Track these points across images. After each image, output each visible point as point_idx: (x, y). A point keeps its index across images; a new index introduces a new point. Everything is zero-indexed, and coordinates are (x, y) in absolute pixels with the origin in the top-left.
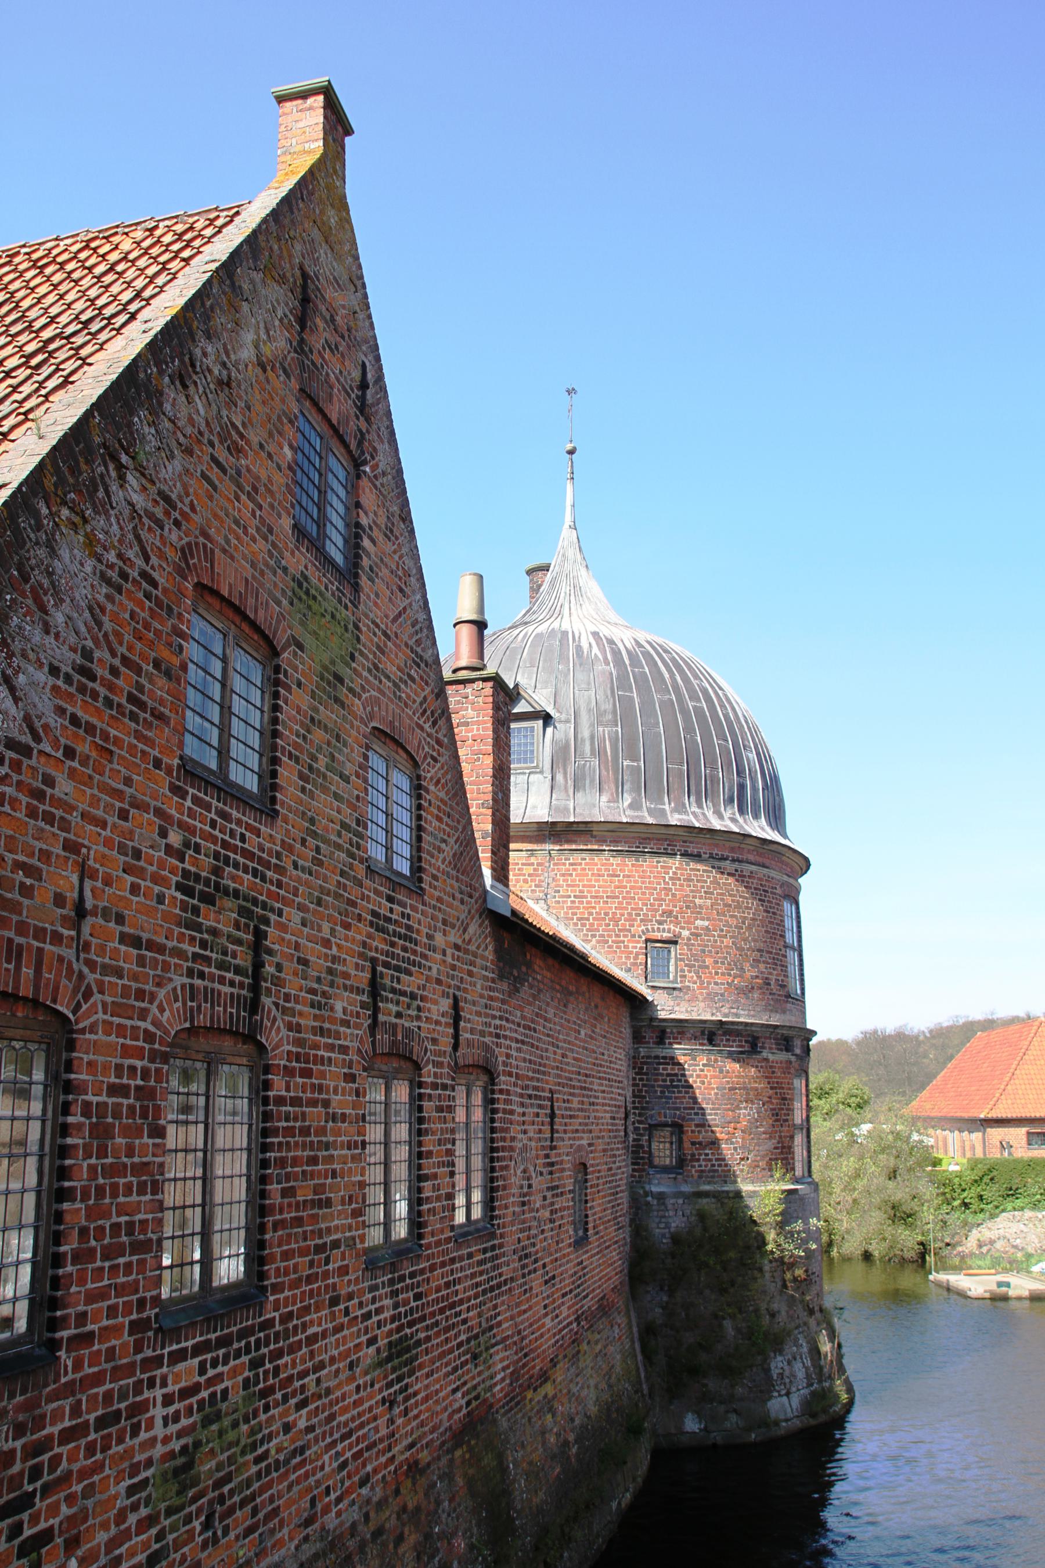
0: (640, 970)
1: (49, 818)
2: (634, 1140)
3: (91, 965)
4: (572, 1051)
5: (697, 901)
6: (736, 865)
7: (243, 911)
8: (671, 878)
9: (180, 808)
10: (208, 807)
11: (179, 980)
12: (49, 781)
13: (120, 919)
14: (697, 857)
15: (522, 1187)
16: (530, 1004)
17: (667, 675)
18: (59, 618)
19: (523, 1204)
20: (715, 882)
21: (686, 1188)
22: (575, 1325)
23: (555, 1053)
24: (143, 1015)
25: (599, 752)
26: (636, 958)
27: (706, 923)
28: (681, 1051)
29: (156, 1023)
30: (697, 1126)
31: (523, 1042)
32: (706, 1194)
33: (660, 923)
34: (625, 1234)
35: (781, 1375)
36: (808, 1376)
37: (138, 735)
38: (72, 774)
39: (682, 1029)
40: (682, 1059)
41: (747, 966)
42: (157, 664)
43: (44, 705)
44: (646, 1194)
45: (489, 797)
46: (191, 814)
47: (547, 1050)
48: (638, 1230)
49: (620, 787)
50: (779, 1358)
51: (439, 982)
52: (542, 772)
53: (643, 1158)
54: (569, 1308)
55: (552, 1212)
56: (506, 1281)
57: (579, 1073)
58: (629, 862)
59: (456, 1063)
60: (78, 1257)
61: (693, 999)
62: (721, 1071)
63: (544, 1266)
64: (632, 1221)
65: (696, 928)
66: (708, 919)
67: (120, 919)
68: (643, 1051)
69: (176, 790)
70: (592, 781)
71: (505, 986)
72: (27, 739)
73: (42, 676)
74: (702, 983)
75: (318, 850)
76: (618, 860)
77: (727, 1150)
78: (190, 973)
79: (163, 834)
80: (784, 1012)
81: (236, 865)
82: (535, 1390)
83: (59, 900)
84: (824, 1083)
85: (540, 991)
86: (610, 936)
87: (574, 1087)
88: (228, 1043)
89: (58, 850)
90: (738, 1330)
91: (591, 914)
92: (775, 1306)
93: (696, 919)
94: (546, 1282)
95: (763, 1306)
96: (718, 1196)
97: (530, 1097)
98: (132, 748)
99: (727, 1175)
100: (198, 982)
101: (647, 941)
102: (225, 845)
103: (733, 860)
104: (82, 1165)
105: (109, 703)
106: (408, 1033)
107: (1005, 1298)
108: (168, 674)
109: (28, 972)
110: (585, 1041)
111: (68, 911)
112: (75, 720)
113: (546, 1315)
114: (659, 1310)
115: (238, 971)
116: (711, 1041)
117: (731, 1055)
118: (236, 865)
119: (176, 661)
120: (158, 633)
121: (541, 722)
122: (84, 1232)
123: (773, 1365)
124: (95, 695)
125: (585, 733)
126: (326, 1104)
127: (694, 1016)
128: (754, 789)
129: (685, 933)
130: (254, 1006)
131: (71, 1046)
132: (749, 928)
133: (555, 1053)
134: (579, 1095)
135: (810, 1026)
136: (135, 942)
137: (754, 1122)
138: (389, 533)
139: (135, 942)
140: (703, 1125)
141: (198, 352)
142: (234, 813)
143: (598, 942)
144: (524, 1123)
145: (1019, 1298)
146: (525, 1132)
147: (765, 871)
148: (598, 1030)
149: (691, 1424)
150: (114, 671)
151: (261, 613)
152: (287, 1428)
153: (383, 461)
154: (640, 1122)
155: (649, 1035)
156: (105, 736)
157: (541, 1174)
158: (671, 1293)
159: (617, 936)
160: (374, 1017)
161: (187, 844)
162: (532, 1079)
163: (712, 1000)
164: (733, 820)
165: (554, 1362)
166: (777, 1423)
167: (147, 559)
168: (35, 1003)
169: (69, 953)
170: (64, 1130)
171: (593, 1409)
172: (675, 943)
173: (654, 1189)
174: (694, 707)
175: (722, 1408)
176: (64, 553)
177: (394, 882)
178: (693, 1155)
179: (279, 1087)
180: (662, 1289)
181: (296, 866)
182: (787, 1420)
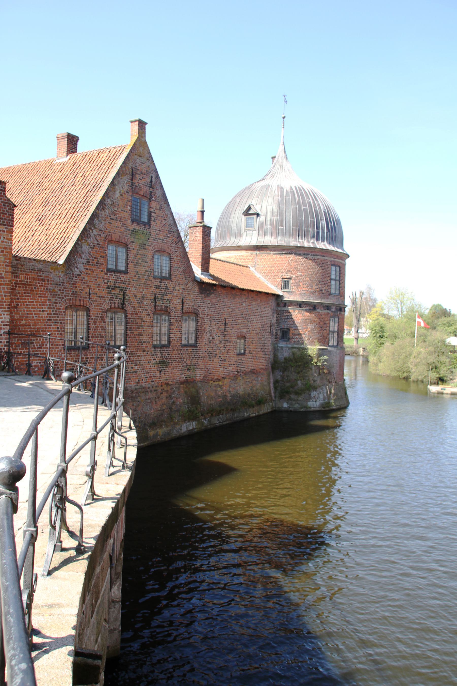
0: (280, 286)
1: (84, 283)
3: (92, 301)
5: (298, 267)
6: (313, 256)
7: (120, 290)
9: (107, 277)
10: (112, 275)
11: (107, 301)
12: (84, 278)
13: (96, 294)
14: (299, 255)
17: (297, 198)
18: (83, 256)
20: (305, 262)
21: (290, 346)
24: (101, 306)
25: (272, 224)
26: (279, 283)
27: (301, 273)
28: (290, 309)
29: (104, 307)
32: (295, 348)
33: (286, 273)
35: (315, 397)
36: (324, 398)
37: (98, 268)
38: (87, 276)
39: (291, 303)
40: (291, 311)
41: (314, 286)
42: (101, 257)
43: (82, 269)
44: (278, 347)
45: (201, 254)
46: (109, 277)
48: (275, 356)
49: (278, 234)
50: (315, 392)
51: (177, 296)
58: (278, 256)
59: (183, 312)
60: (91, 337)
61: (296, 294)
62: (303, 315)
64: (274, 353)
67: (96, 294)
68: (279, 309)
69: (105, 274)
70: (270, 233)
71: (203, 295)
72: (80, 273)
73: (82, 265)
75: (139, 277)
76: (275, 256)
77: (304, 336)
78: (110, 300)
79: (104, 281)
80: (328, 299)
81: (119, 283)
83: (86, 293)
84: (450, 321)
88: (118, 310)
89: (86, 287)
90: (303, 384)
92: (315, 379)
95: (311, 379)
96: (299, 349)
98: (97, 270)
99: (303, 343)
100: (111, 301)
101: (282, 278)
102: (116, 280)
103: (312, 255)
104: (92, 327)
105: (93, 265)
106: (167, 307)
107: (442, 393)
108: (103, 257)
109: (82, 302)
111: (88, 294)
112: (87, 269)
114: (279, 377)
115: (120, 299)
116: (300, 307)
117: (306, 311)
118: (119, 283)
119: (105, 255)
120: (101, 252)
121: (256, 216)
122: (92, 334)
123: (312, 394)
124: (90, 265)
125: (269, 218)
126: (142, 319)
127: (295, 300)
128: (323, 232)
129: (294, 276)
130: (123, 304)
131: (89, 311)
132: (316, 275)
136: (100, 297)
137: (313, 330)
138: (161, 208)
139: (100, 297)
140: (296, 328)
141: (106, 202)
142: (118, 275)
145: (447, 394)
147: (323, 258)
149: (285, 405)
150: (93, 260)
151: (123, 240)
152: (132, 368)
153: (158, 193)
155: (282, 304)
156: (92, 270)
158: (283, 372)
160: (155, 304)
161: (108, 282)
163: (301, 295)
164: (313, 243)
166: (310, 408)
167: (98, 241)
168: (84, 306)
169: (88, 299)
170: (89, 321)
172: (291, 279)
173: (280, 345)
174: (304, 209)
175: (294, 402)
176: (84, 247)
177: (162, 279)
179: (129, 316)
180: (281, 371)
181: (133, 280)
182: (314, 407)
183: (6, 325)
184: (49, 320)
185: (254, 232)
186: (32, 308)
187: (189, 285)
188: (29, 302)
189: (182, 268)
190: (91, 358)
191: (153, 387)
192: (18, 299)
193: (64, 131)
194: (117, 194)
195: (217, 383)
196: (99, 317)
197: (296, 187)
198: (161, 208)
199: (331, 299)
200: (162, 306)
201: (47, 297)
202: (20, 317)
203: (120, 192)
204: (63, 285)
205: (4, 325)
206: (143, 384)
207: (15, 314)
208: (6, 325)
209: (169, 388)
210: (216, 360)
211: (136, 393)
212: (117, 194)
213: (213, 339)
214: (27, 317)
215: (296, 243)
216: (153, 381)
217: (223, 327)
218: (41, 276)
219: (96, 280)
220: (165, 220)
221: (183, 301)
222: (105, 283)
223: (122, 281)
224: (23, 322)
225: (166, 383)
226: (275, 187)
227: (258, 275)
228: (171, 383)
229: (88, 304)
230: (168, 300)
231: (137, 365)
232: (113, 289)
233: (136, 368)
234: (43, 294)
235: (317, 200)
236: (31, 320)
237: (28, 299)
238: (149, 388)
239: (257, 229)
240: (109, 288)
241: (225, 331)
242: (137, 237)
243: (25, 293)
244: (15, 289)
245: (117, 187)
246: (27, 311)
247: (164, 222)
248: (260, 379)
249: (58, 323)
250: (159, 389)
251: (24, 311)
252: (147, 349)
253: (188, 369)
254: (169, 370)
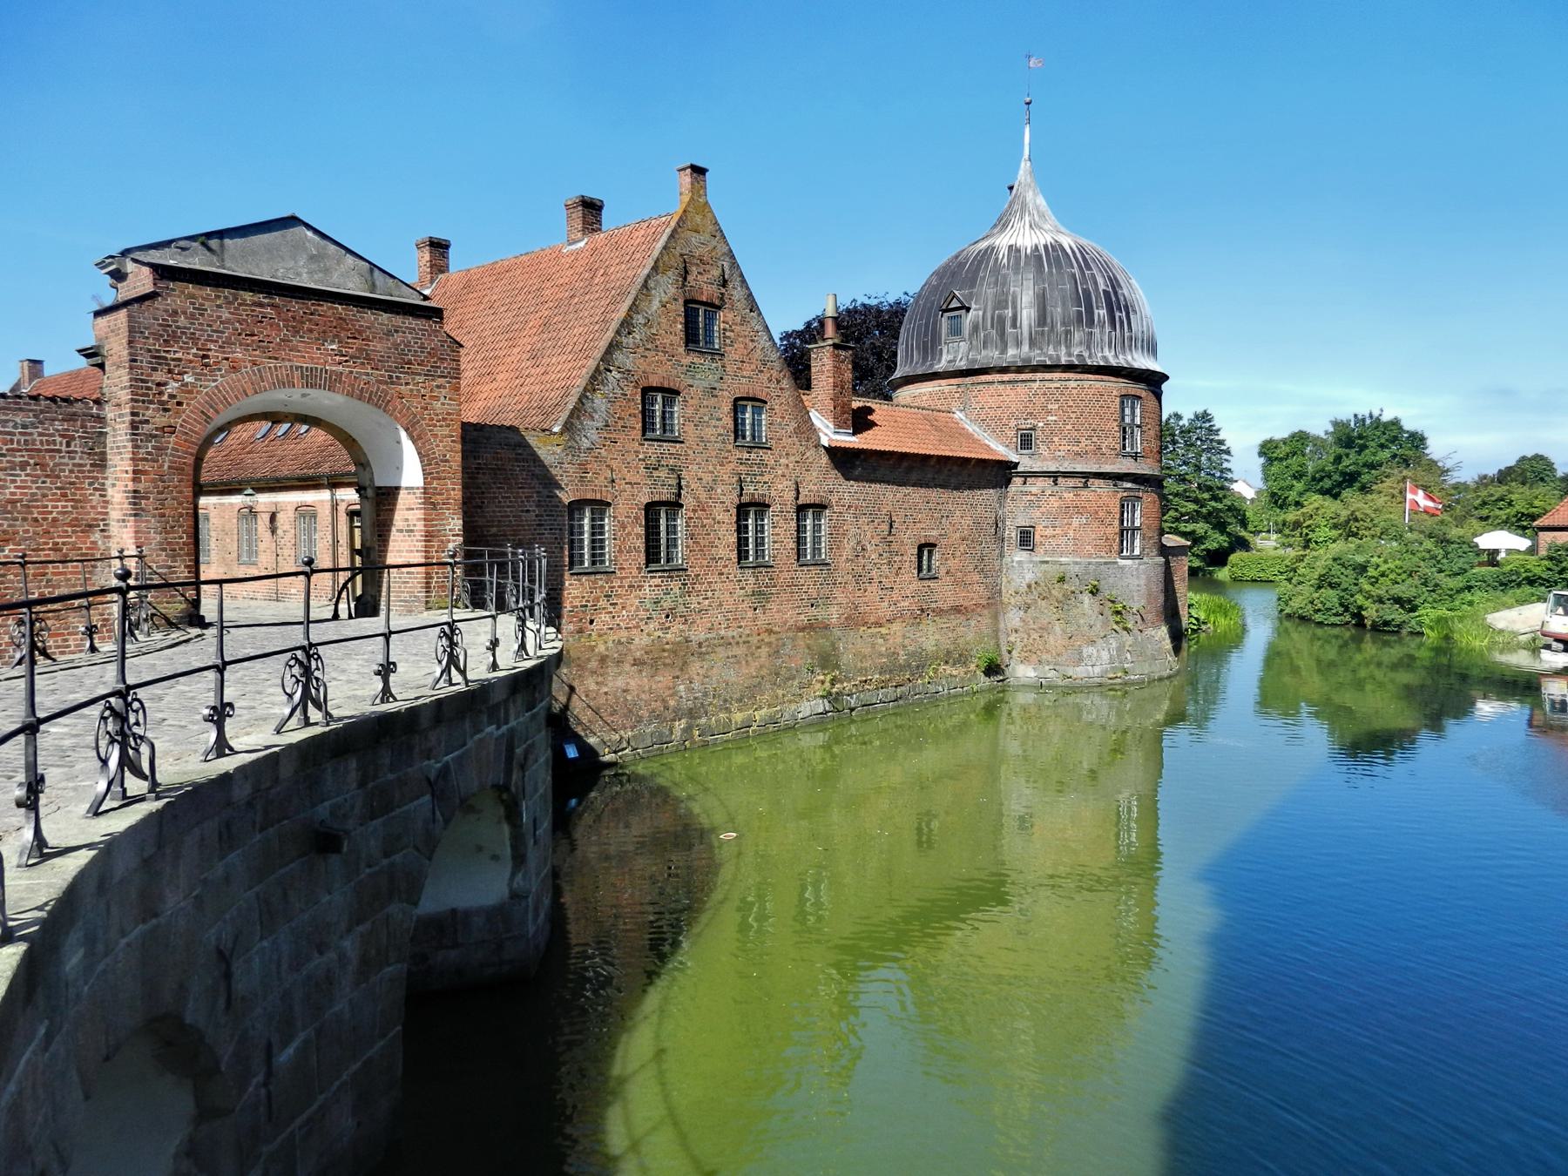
0: (1013, 445)
6: (1078, 382)
27: (1054, 418)
33: (1025, 419)
51: (783, 476)
83: (606, 478)
126: (714, 519)
130: (679, 495)
136: (630, 483)
139: (630, 483)
152: (699, 603)
173: (1016, 559)
183: (458, 535)
184: (538, 525)
185: (961, 344)
186: (508, 507)
187: (808, 454)
188: (503, 497)
189: (793, 425)
190: (619, 587)
191: (740, 637)
192: (483, 493)
193: (573, 194)
194: (656, 304)
195: (878, 630)
196: (630, 517)
197: (1046, 247)
198: (744, 321)
199: (1121, 463)
200: (753, 494)
201: (534, 488)
202: (488, 522)
203: (660, 302)
204: (561, 468)
205: (453, 535)
206: (722, 632)
207: (479, 517)
208: (458, 535)
209: (773, 638)
210: (874, 588)
211: (708, 646)
212: (656, 304)
213: (863, 549)
214: (499, 521)
215: (1042, 359)
216: (740, 627)
217: (885, 527)
218: (520, 454)
219: (623, 455)
220: (752, 341)
221: (797, 483)
222: (640, 460)
223: (673, 454)
224: (494, 530)
225: (767, 630)
226: (1004, 251)
227: (971, 428)
228: (776, 629)
229: (609, 496)
230: (765, 483)
231: (707, 599)
232: (657, 469)
233: (707, 602)
234: (526, 483)
235: (1089, 268)
236: (508, 526)
237: (500, 493)
238: (733, 637)
239: (967, 337)
240: (649, 468)
242: (698, 376)
243: (495, 483)
244: (477, 478)
245: (653, 292)
246: (500, 512)
247: (751, 345)
248: (973, 623)
249: (556, 529)
250: (754, 640)
251: (494, 512)
252: (725, 570)
253: (812, 606)
254: (773, 606)
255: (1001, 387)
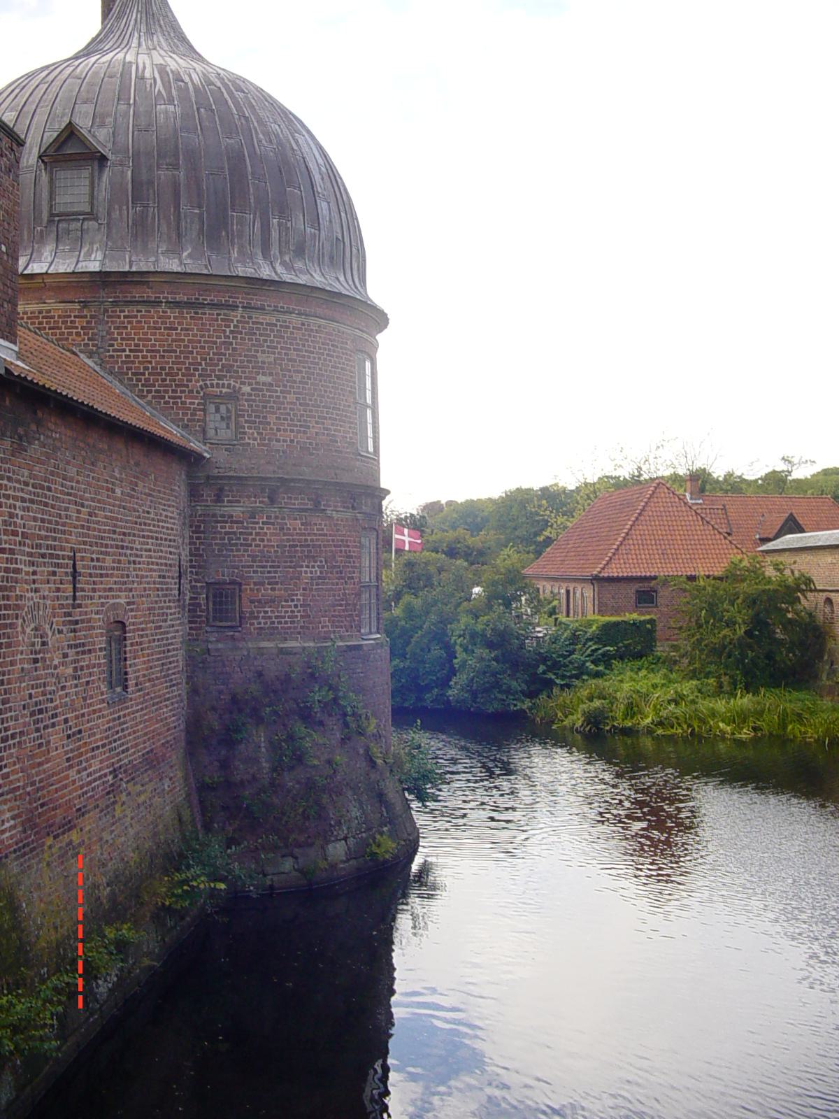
2: (191, 599)
4: (101, 509)
6: (303, 319)
8: (231, 332)
15: (33, 644)
16: (40, 462)
19: (36, 661)
22: (110, 777)
23: (79, 512)
27: (269, 379)
30: (255, 584)
31: (32, 501)
33: (219, 378)
34: (182, 691)
47: (67, 509)
52: (96, 219)
53: (200, 616)
54: (102, 762)
55: (75, 669)
56: (13, 736)
57: (114, 532)
63: (66, 721)
65: (258, 383)
66: (271, 374)
74: (263, 439)
82: (55, 837)
85: (55, 449)
86: (166, 392)
87: (107, 546)
91: (147, 368)
93: (258, 373)
94: (69, 737)
97: (43, 556)
110: (121, 500)
113: (71, 767)
133: (79, 512)
134: (114, 554)
135: (383, 485)
143: (154, 397)
144: (34, 582)
146: (36, 591)
148: (139, 488)
154: (196, 581)
157: (60, 632)
159: (173, 391)
162: (46, 538)
165: (81, 812)
171: (133, 856)
178: (252, 613)
213: (44, 644)
241: (74, 607)
255: (172, 314)
